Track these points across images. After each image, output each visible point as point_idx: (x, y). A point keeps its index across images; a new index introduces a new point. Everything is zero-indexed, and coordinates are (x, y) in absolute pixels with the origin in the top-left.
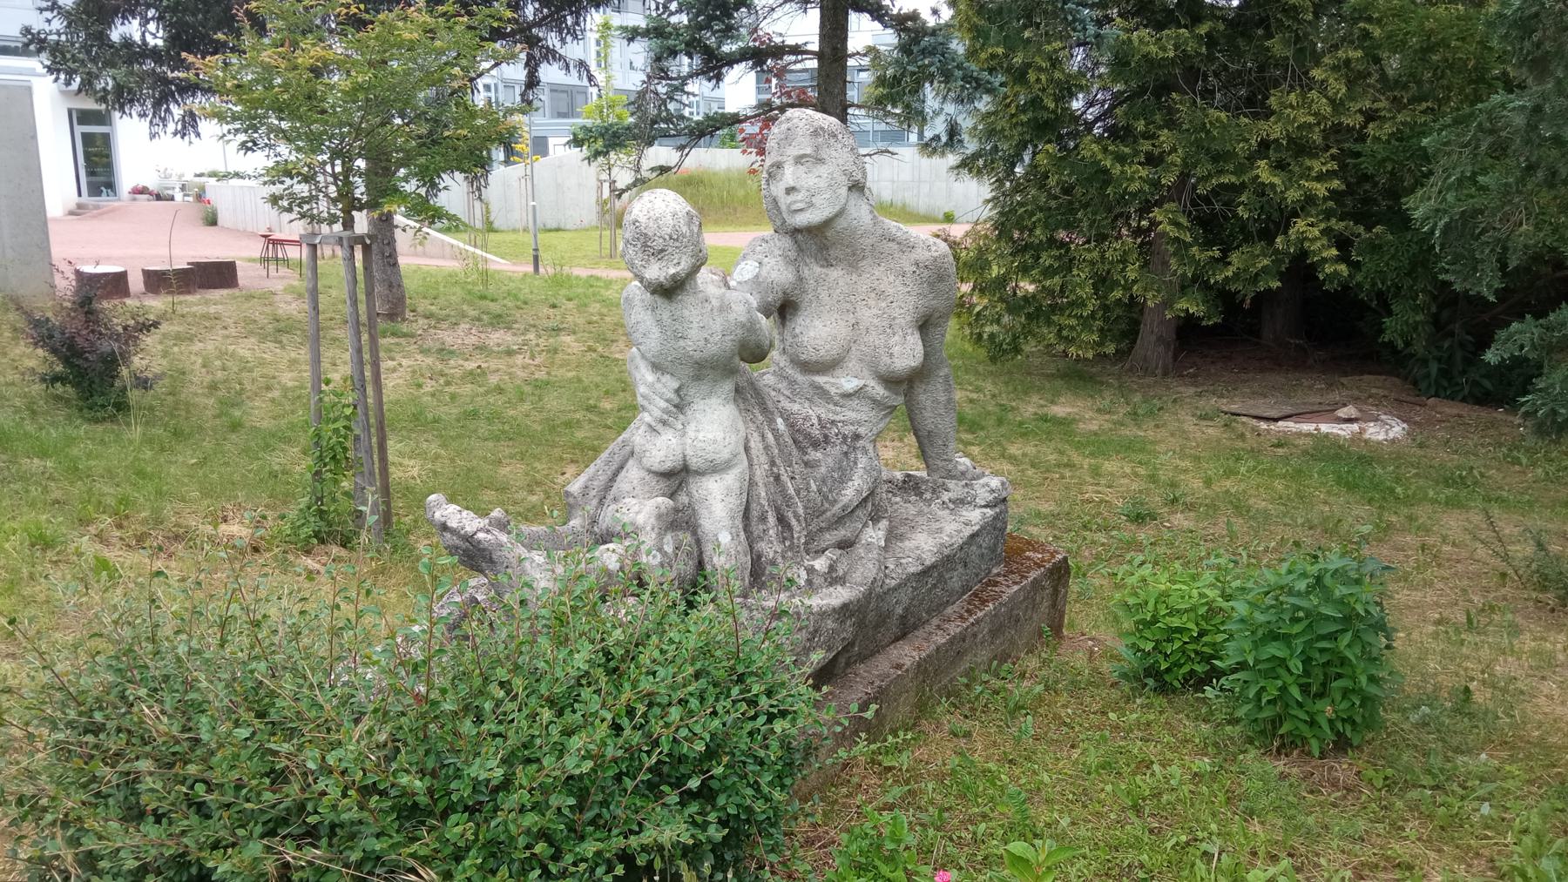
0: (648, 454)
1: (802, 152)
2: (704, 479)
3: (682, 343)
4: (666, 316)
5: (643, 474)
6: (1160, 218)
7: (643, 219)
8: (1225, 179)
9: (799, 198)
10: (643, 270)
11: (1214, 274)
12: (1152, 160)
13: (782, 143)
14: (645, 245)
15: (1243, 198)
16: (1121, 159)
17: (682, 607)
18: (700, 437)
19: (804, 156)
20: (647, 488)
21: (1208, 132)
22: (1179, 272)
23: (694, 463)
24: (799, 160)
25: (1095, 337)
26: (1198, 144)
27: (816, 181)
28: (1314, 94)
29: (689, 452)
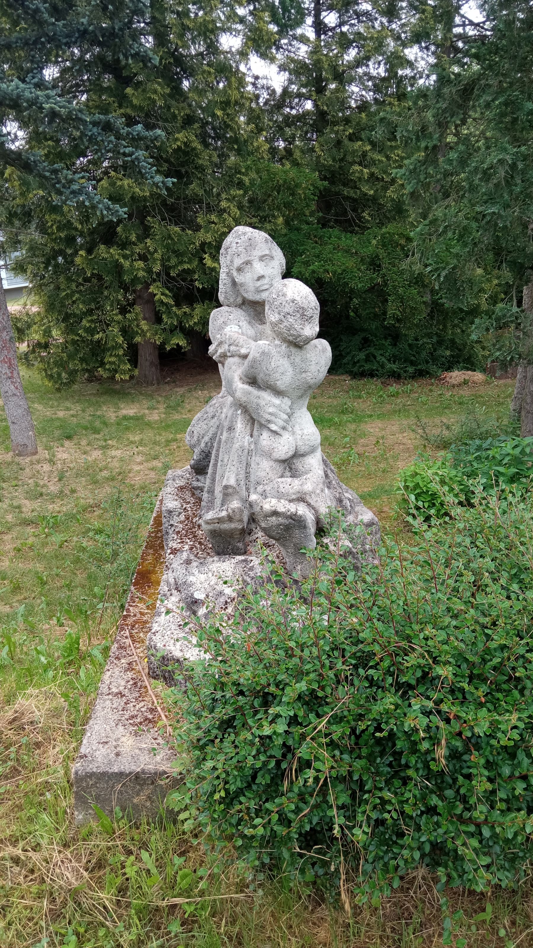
0: (276, 450)
1: (264, 253)
2: (305, 458)
3: (304, 375)
4: (298, 360)
5: (272, 463)
6: (155, 292)
7: (298, 298)
8: (186, 266)
9: (266, 282)
10: (301, 331)
11: (188, 322)
12: (143, 257)
13: (248, 248)
14: (303, 315)
15: (196, 277)
16: (125, 257)
17: (447, 519)
18: (305, 432)
19: (266, 255)
20: (275, 472)
21: (172, 239)
22: (169, 322)
23: (303, 449)
24: (262, 258)
25: (129, 366)
26: (167, 247)
27: (272, 270)
28: (225, 215)
29: (300, 443)
